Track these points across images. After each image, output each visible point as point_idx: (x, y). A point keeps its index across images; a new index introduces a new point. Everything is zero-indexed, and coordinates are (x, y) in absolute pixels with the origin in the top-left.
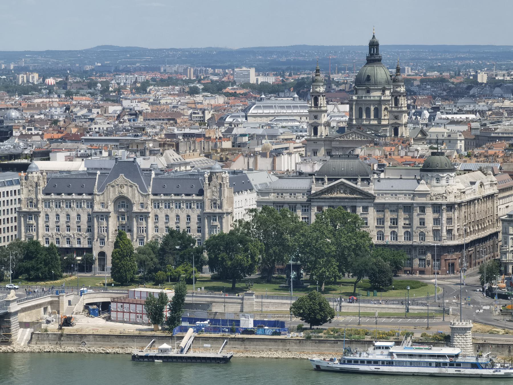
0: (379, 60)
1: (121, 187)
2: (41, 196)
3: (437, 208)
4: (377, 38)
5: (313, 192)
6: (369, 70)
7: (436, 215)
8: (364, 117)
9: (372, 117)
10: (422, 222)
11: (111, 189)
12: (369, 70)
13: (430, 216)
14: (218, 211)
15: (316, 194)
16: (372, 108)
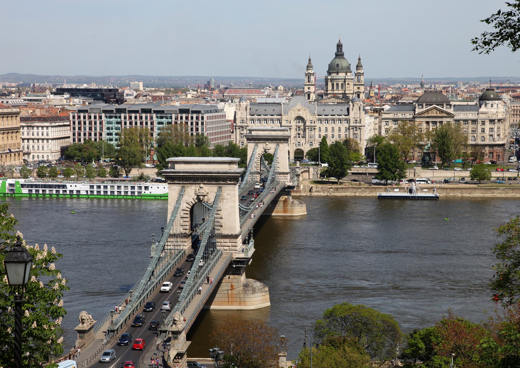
0: (343, 55)
1: (299, 110)
2: (249, 117)
3: (492, 121)
4: (342, 42)
6: (338, 61)
8: (335, 89)
9: (340, 88)
10: (483, 131)
11: (293, 112)
13: (488, 126)
14: (358, 125)
15: (419, 114)
16: (340, 83)
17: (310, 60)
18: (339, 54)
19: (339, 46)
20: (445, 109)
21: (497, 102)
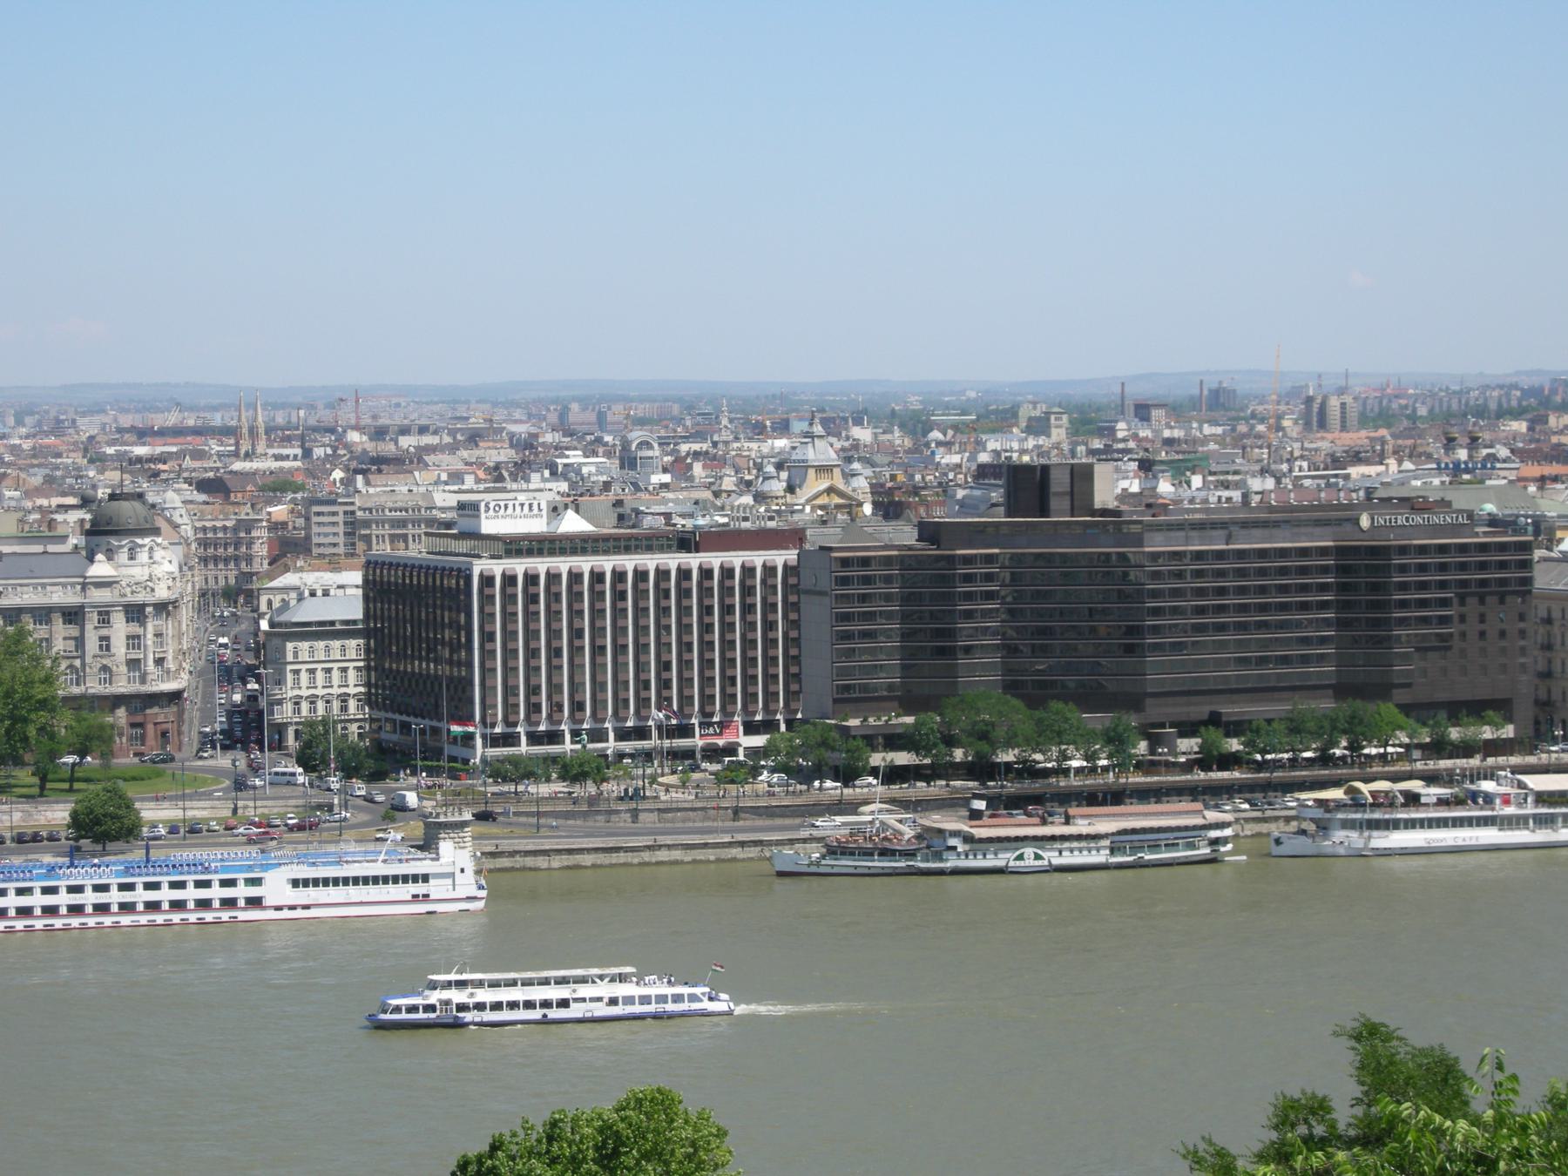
3: (135, 613)
7: (135, 628)
13: (120, 628)
21: (147, 540)
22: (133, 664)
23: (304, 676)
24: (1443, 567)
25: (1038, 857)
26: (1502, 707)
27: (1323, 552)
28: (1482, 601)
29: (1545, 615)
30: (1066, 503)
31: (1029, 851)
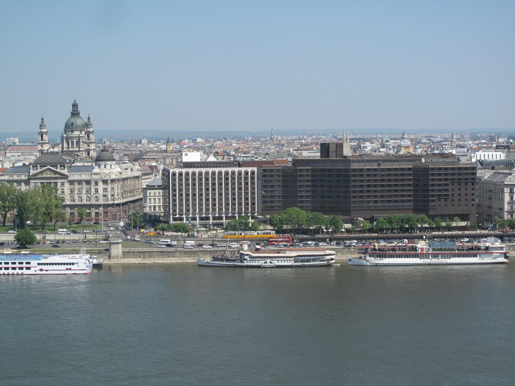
3: (105, 182)
4: (77, 102)
5: (31, 174)
6: (73, 120)
8: (70, 146)
10: (97, 191)
12: (73, 120)
15: (33, 175)
16: (75, 141)
17: (42, 120)
18: (75, 113)
19: (75, 106)
20: (58, 170)
21: (109, 162)
22: (105, 196)
23: (152, 200)
24: (446, 174)
25: (271, 262)
26: (464, 217)
27: (409, 169)
28: (466, 184)
29: (490, 189)
30: (335, 154)
31: (268, 261)
